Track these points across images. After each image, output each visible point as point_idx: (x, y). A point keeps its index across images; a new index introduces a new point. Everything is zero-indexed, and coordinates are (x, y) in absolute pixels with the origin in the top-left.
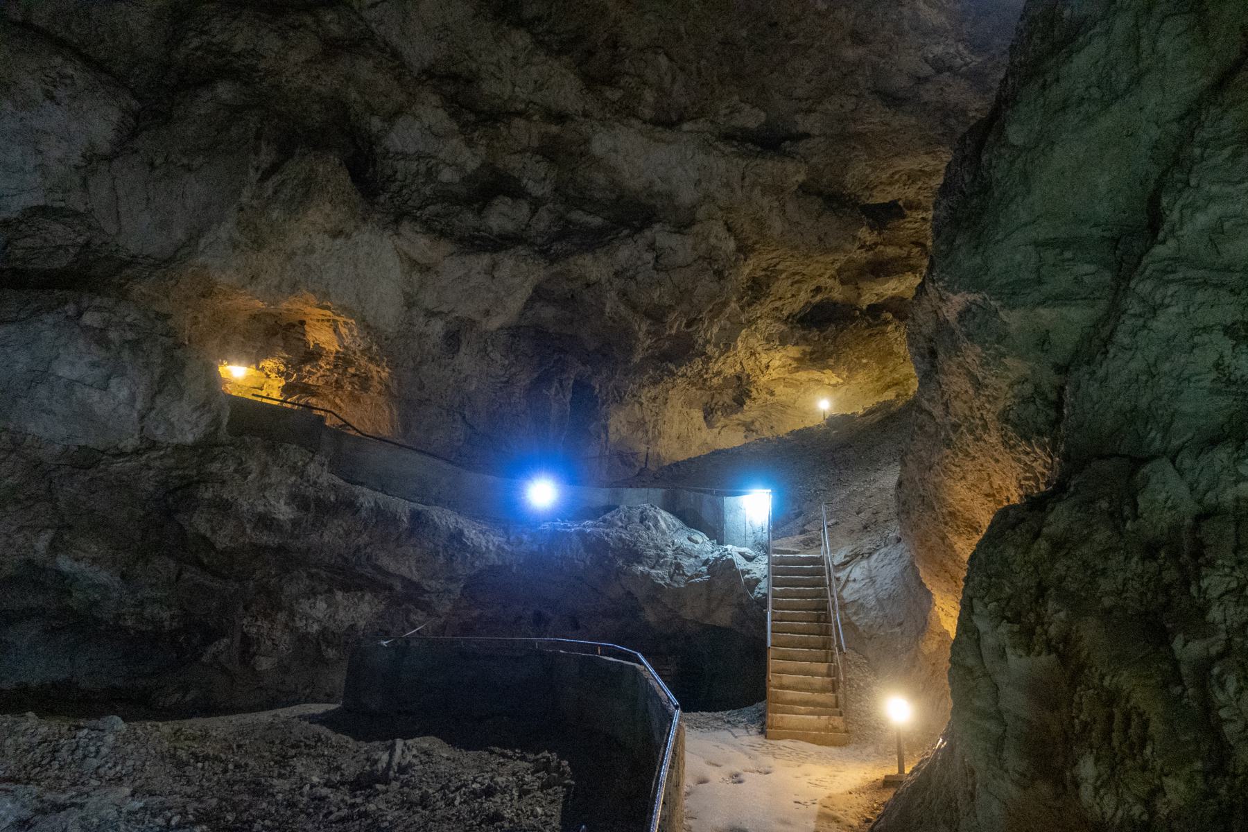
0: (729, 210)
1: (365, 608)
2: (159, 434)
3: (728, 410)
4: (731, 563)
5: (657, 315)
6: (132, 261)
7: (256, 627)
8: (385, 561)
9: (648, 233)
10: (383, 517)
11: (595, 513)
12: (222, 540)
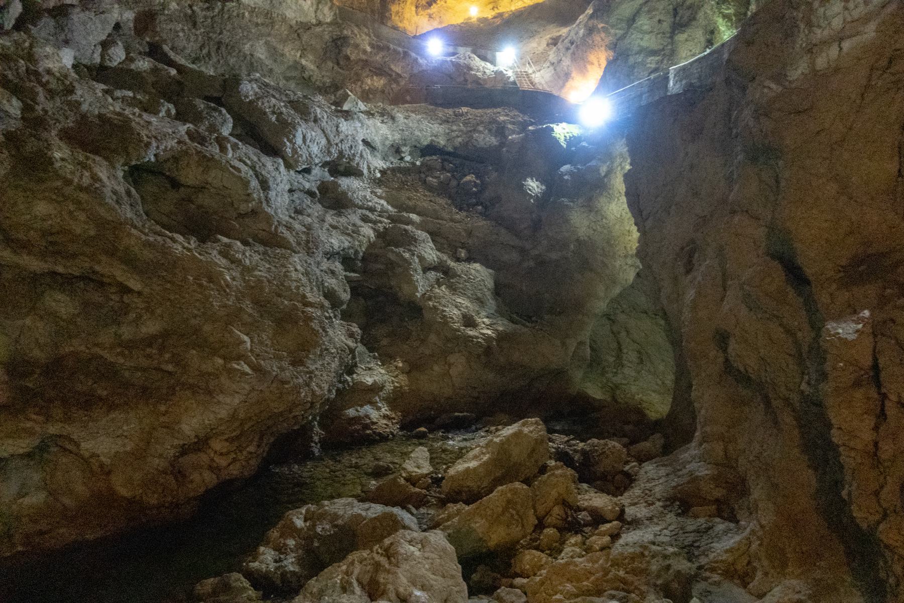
1: (382, 82)
4: (501, 72)
8: (392, 67)
10: (396, 52)
11: (454, 54)
12: (353, 57)
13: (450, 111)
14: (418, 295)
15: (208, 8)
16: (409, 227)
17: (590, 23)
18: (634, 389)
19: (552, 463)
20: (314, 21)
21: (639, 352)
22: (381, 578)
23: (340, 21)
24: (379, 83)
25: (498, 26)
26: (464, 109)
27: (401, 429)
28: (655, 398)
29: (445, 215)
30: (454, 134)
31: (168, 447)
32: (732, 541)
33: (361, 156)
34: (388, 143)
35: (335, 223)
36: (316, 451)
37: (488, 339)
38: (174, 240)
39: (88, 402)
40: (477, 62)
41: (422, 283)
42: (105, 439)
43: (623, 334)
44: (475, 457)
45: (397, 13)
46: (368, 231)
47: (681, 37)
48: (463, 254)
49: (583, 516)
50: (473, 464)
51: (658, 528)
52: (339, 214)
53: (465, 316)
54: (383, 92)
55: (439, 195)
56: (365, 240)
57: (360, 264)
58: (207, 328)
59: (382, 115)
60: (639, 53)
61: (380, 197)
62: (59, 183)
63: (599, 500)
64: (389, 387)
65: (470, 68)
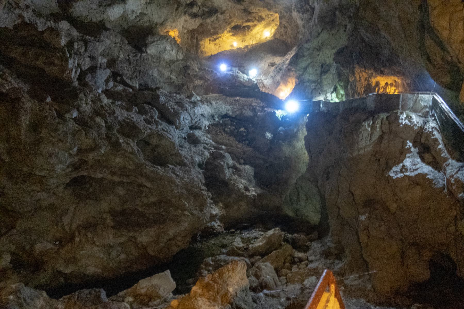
0: (230, 12)
2: (178, 57)
3: (213, 41)
5: (215, 29)
6: (156, 24)
7: (188, 84)
8: (206, 76)
9: (217, 14)
12: (191, 74)
13: (232, 99)
14: (226, 178)
15: (135, 56)
16: (222, 151)
17: (289, 67)
18: (304, 211)
19: (283, 243)
20: (176, 59)
21: (306, 195)
22: (258, 273)
23: (186, 59)
24: (200, 82)
25: (246, 53)
26: (238, 98)
27: (225, 230)
28: (313, 214)
29: (234, 145)
30: (235, 110)
31: (164, 239)
32: (340, 266)
33: (202, 122)
34: (210, 114)
35: (195, 151)
36: (199, 239)
37: (254, 196)
38: (158, 169)
39: (140, 225)
40: (241, 74)
41: (228, 173)
42: (144, 237)
43: (300, 189)
44: (260, 241)
45: (202, 44)
46: (206, 153)
47: (324, 77)
48: (242, 161)
49: (296, 260)
50: (260, 244)
51: (319, 263)
52: (196, 147)
53: (245, 187)
54: (201, 86)
55: (230, 136)
56: (206, 157)
57: (204, 166)
58: (174, 200)
59: (207, 102)
60: (308, 82)
61: (210, 139)
62: (124, 152)
63: (301, 255)
64: (220, 215)
65: (238, 77)
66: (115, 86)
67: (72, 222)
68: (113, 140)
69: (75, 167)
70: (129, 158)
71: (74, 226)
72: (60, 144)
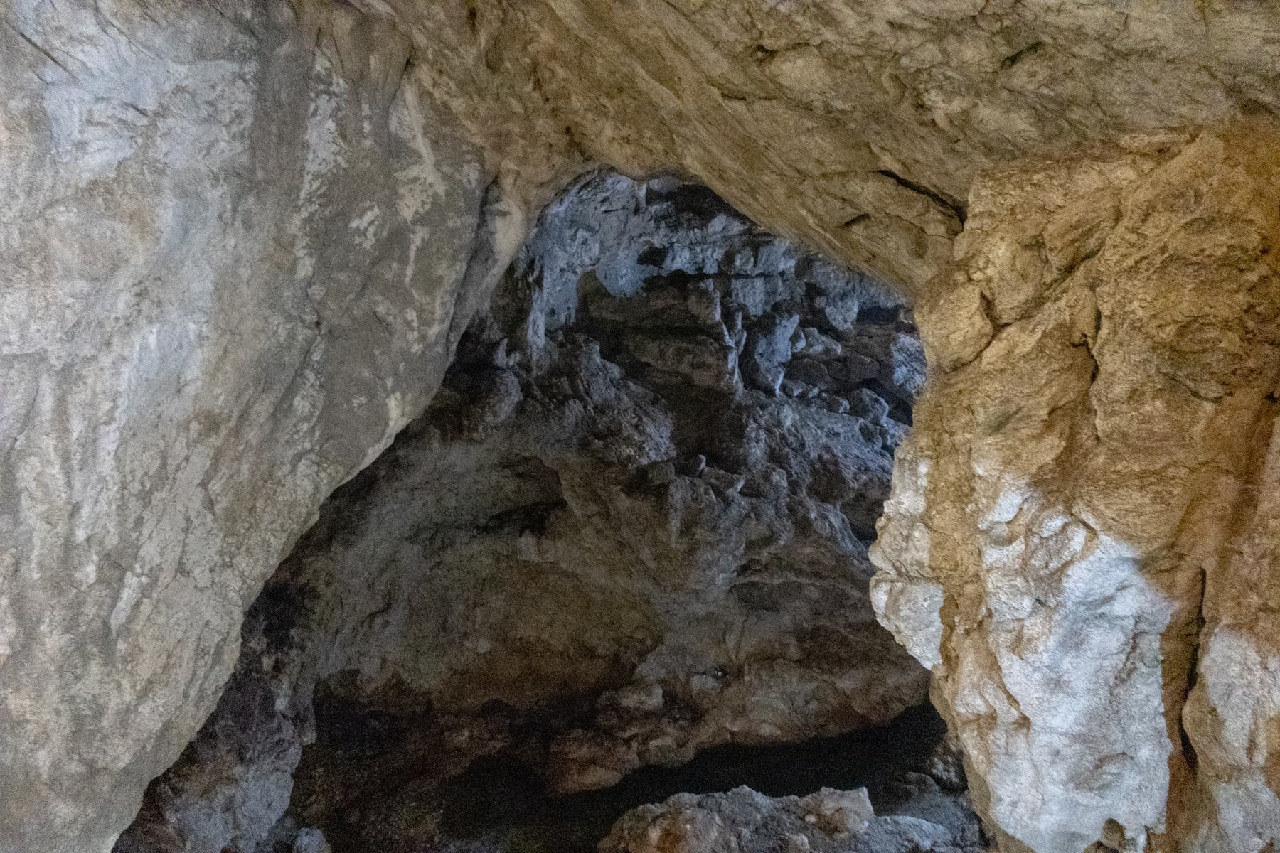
42: (848, 682)
62: (815, 537)
66: (809, 345)
67: (738, 646)
68: (800, 515)
69: (743, 570)
70: (826, 547)
71: (742, 654)
72: (722, 546)
